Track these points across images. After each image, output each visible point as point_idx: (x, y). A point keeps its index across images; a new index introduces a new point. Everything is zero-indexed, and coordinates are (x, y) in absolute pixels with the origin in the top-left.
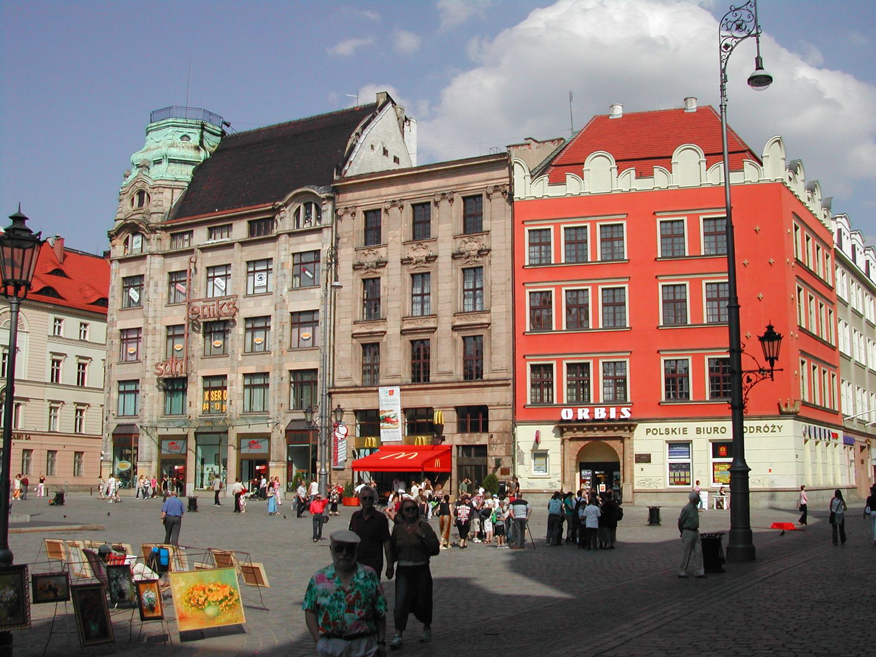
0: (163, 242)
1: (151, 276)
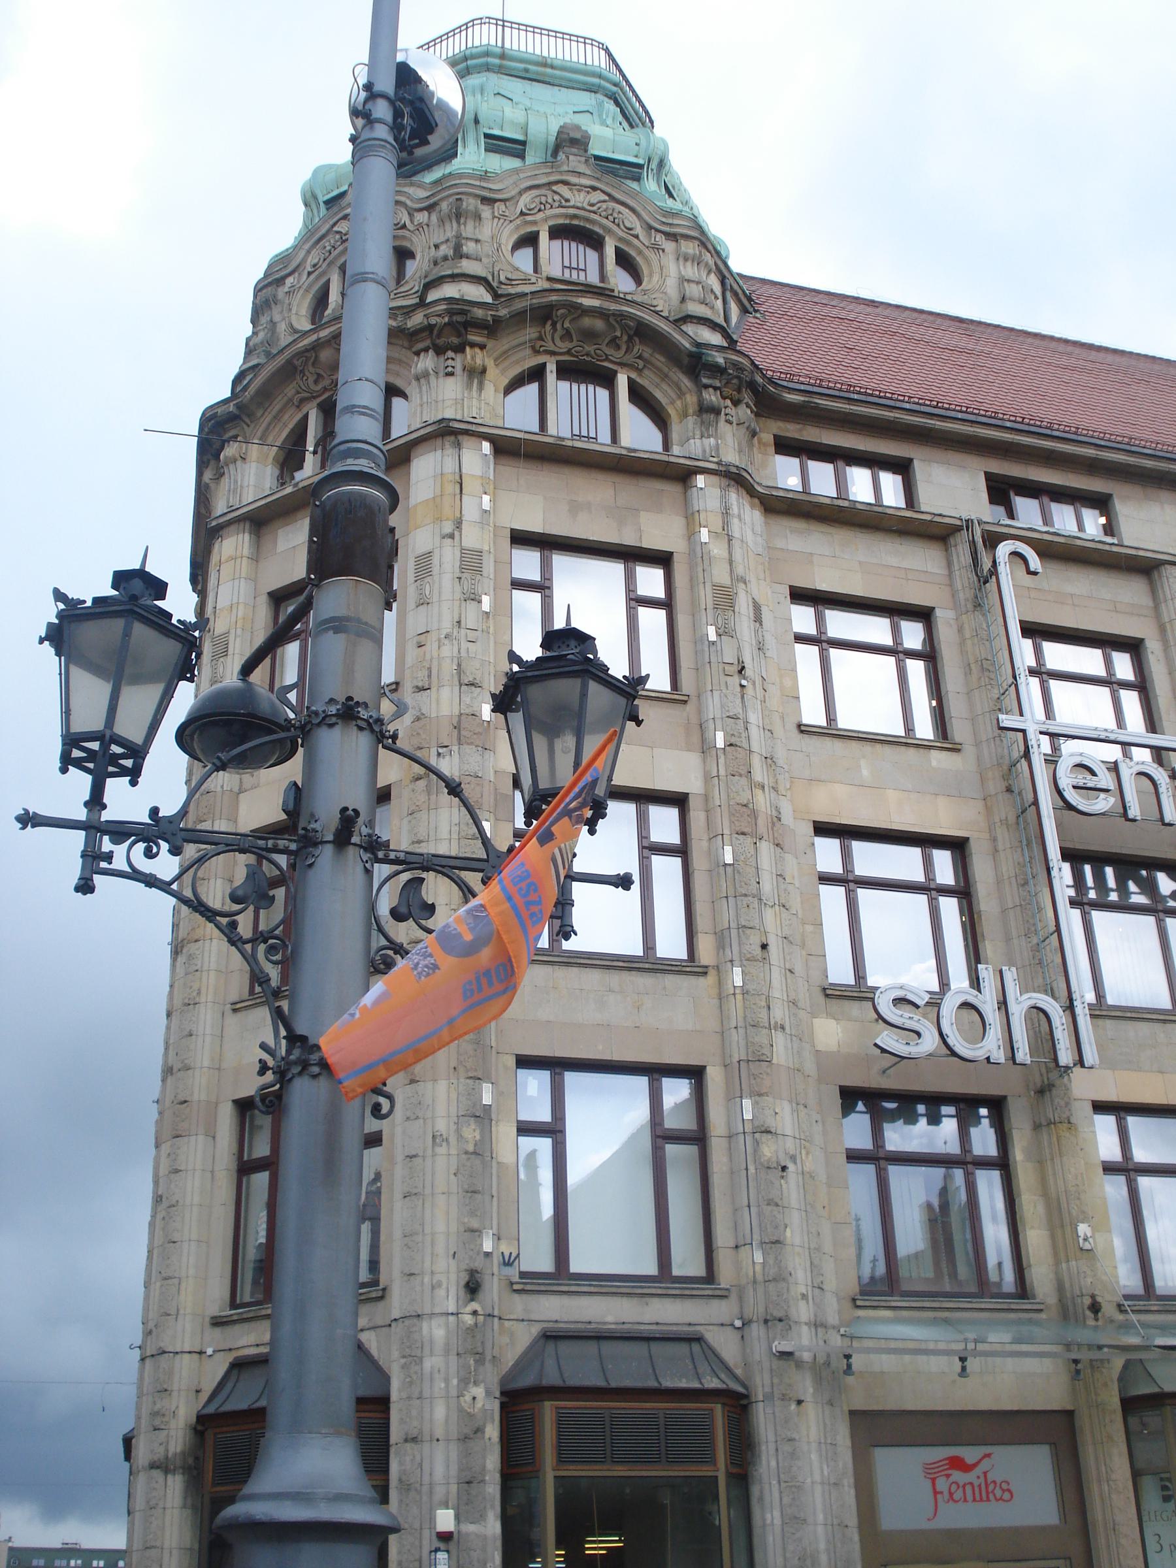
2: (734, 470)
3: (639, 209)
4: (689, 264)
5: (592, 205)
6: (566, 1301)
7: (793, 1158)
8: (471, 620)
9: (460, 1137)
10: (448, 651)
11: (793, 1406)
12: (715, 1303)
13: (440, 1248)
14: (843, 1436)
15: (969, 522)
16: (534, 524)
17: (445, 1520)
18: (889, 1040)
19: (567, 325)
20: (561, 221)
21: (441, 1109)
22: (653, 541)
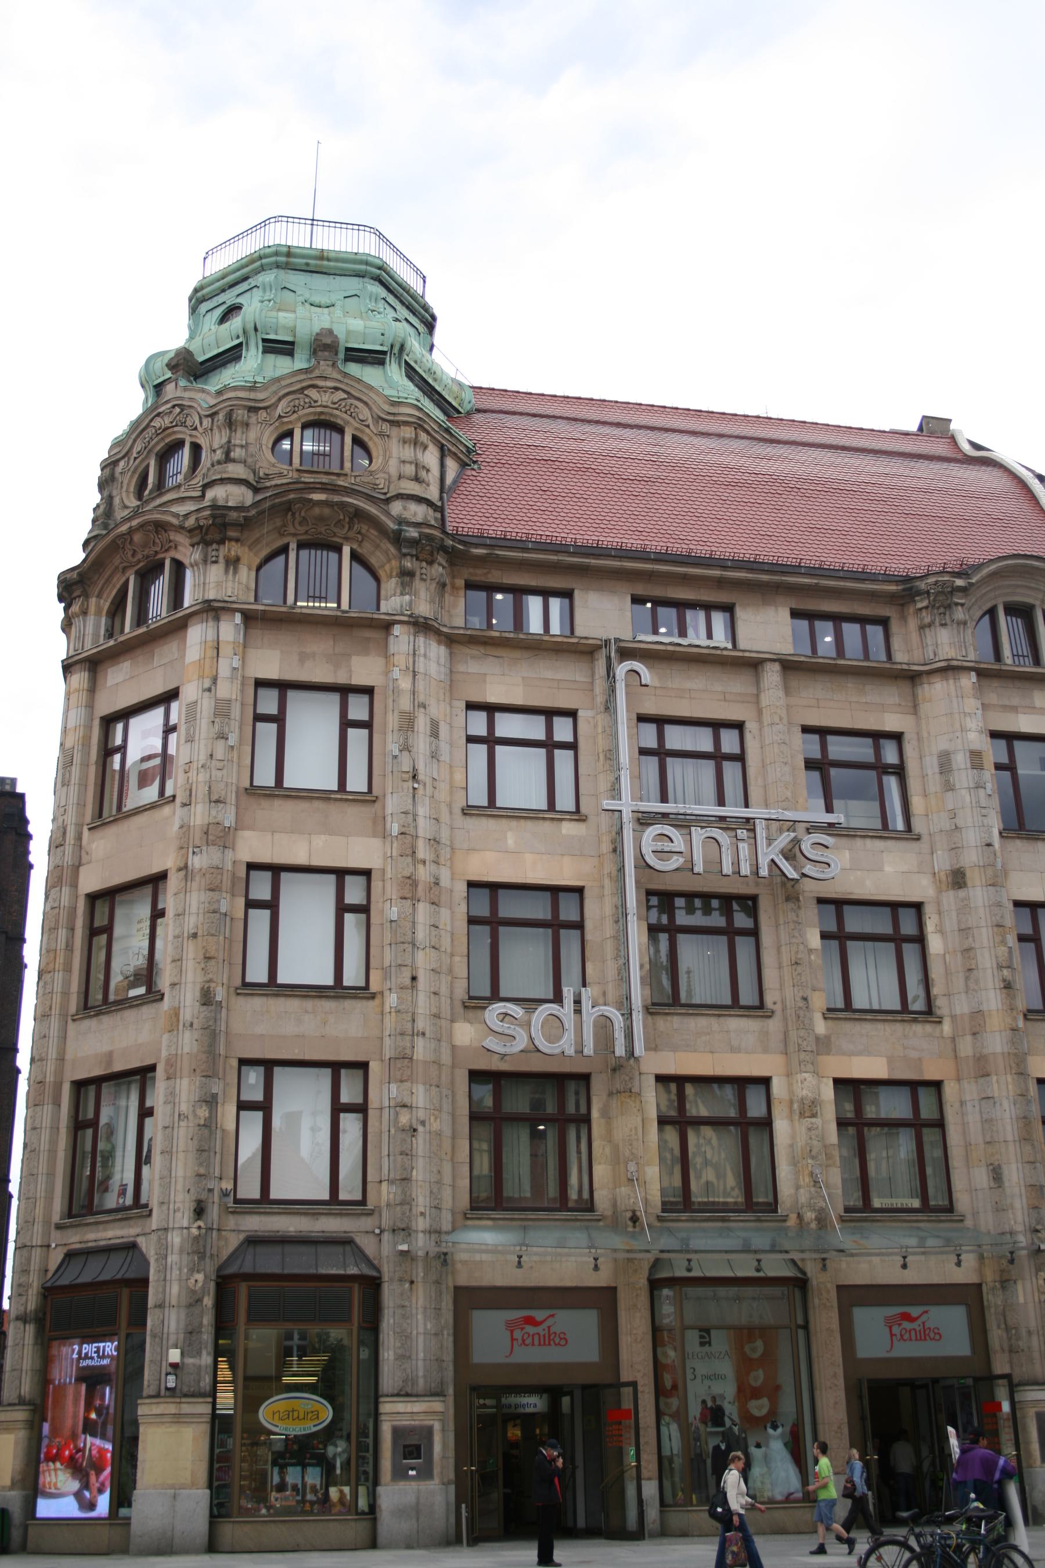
1: (421, 698)
2: (422, 620)
3: (370, 403)
4: (407, 446)
5: (335, 403)
6: (264, 1219)
7: (423, 1123)
8: (219, 753)
9: (195, 1115)
10: (202, 777)
11: (407, 1285)
12: (363, 1219)
13: (180, 1187)
14: (447, 1303)
15: (607, 642)
16: (271, 671)
17: (174, 1355)
18: (491, 1043)
19: (303, 514)
20: (311, 418)
21: (184, 1097)
22: (359, 679)
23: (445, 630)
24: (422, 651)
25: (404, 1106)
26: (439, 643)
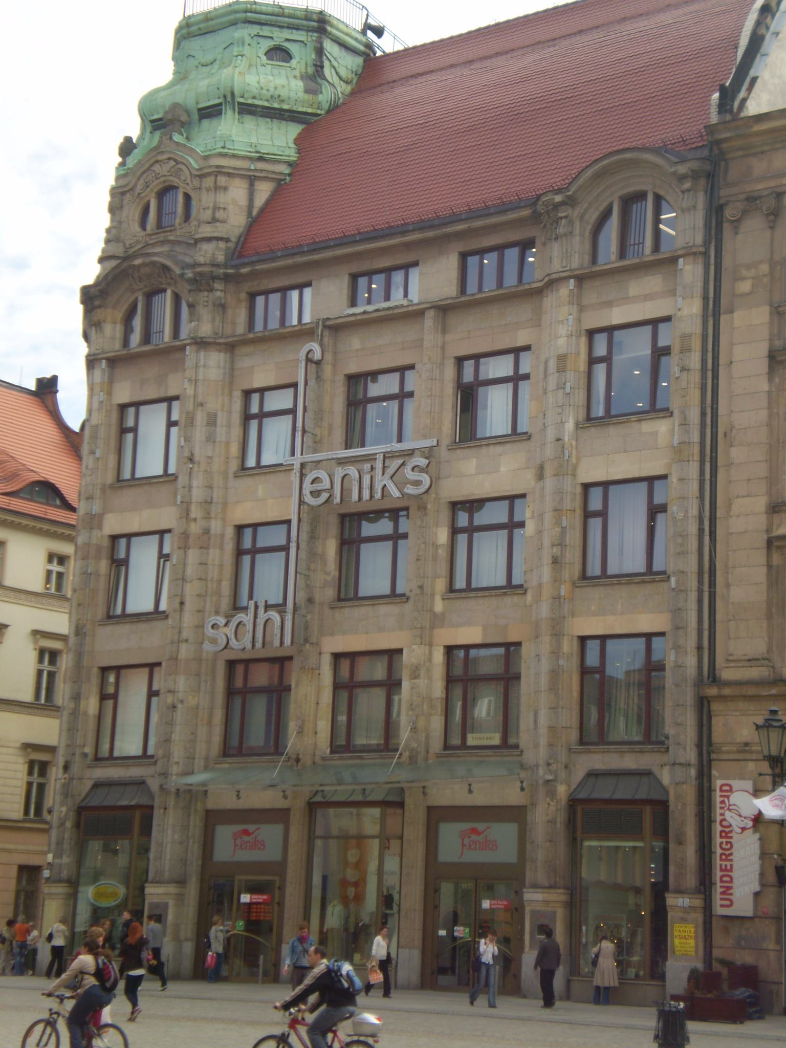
0: (230, 312)
1: (200, 399)
2: (199, 340)
7: (182, 702)
23: (221, 341)
24: (202, 362)
25: (169, 691)
26: (220, 351)
